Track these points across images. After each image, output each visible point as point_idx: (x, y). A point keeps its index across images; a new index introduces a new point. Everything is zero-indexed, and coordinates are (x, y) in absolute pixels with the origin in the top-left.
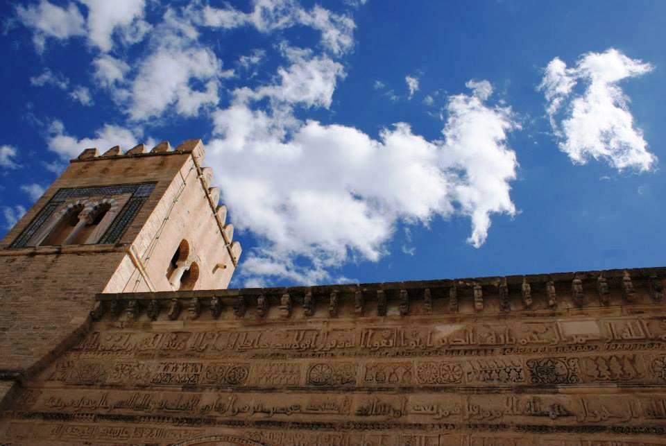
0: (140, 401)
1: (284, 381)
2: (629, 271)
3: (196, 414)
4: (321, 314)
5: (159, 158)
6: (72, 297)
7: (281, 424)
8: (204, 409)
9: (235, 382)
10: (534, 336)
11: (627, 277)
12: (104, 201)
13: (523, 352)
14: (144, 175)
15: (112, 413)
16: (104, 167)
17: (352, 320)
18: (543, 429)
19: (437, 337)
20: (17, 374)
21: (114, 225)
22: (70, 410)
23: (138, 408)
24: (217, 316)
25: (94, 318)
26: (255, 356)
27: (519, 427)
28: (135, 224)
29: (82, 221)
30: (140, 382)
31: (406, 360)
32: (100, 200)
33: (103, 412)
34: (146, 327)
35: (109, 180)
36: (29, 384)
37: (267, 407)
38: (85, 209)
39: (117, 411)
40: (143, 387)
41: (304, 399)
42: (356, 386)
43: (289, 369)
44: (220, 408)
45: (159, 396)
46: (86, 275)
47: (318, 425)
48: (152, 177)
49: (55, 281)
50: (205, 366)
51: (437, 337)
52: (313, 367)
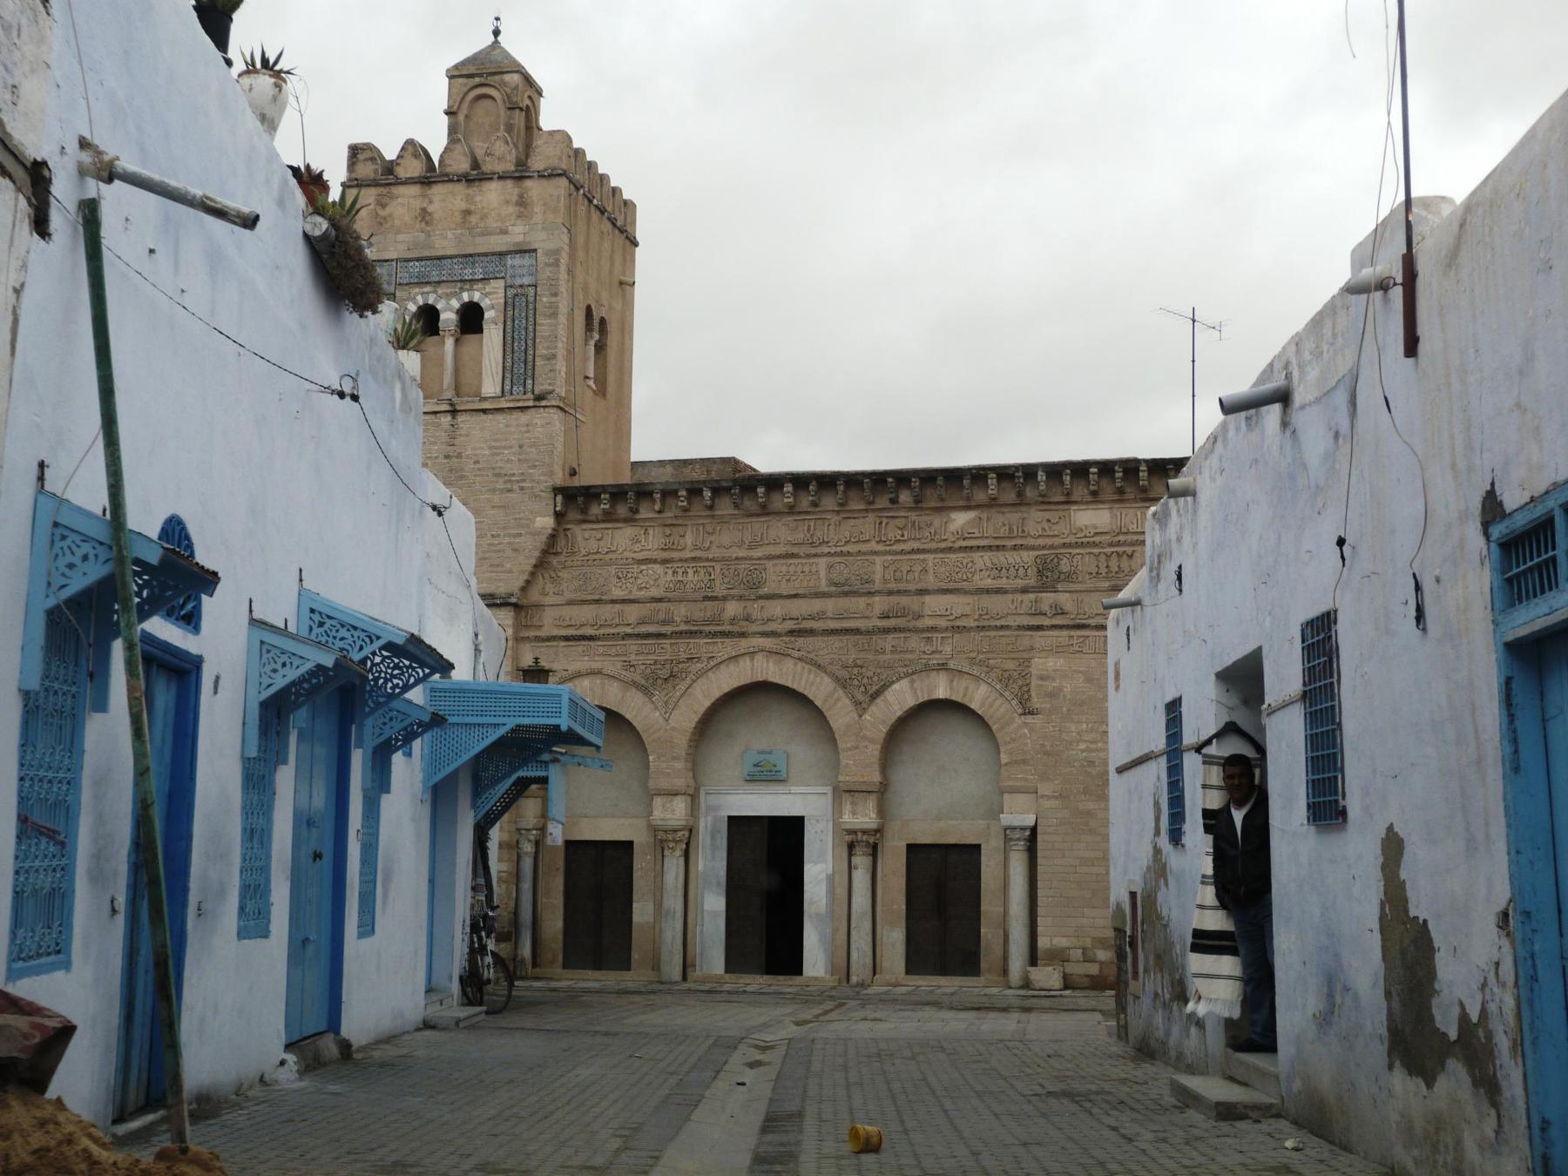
0: (661, 616)
1: (805, 584)
2: (1146, 461)
3: (727, 628)
4: (829, 502)
5: (509, 183)
6: (516, 487)
7: (811, 632)
8: (733, 621)
9: (753, 590)
10: (1046, 525)
11: (1143, 467)
12: (466, 297)
13: (1033, 548)
14: (504, 232)
15: (636, 631)
16: (418, 204)
17: (862, 507)
18: (1039, 628)
19: (952, 527)
20: (513, 600)
21: (509, 350)
22: (589, 631)
23: (665, 622)
24: (711, 508)
25: (559, 516)
26: (770, 557)
27: (1020, 628)
28: (541, 351)
29: (449, 343)
30: (654, 592)
31: (921, 556)
32: (457, 295)
33: (628, 630)
34: (629, 521)
35: (445, 243)
36: (524, 602)
37: (795, 614)
38: (443, 316)
39: (643, 629)
40: (660, 600)
41: (830, 605)
42: (878, 586)
43: (806, 569)
44: (748, 619)
45: (680, 611)
46: (516, 449)
47: (847, 631)
48: (520, 238)
49: (476, 462)
50: (718, 568)
51: (952, 527)
52: (830, 567)
